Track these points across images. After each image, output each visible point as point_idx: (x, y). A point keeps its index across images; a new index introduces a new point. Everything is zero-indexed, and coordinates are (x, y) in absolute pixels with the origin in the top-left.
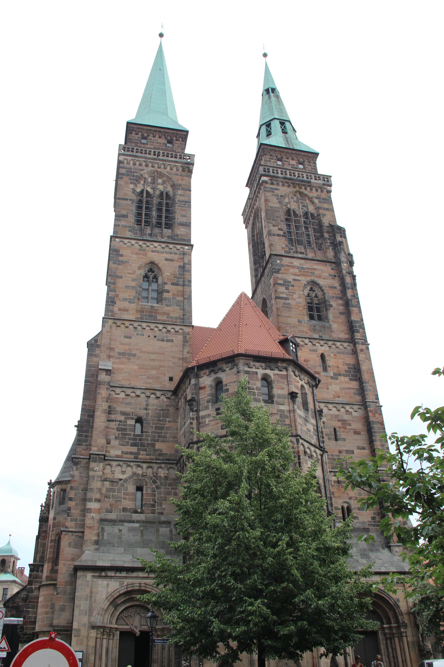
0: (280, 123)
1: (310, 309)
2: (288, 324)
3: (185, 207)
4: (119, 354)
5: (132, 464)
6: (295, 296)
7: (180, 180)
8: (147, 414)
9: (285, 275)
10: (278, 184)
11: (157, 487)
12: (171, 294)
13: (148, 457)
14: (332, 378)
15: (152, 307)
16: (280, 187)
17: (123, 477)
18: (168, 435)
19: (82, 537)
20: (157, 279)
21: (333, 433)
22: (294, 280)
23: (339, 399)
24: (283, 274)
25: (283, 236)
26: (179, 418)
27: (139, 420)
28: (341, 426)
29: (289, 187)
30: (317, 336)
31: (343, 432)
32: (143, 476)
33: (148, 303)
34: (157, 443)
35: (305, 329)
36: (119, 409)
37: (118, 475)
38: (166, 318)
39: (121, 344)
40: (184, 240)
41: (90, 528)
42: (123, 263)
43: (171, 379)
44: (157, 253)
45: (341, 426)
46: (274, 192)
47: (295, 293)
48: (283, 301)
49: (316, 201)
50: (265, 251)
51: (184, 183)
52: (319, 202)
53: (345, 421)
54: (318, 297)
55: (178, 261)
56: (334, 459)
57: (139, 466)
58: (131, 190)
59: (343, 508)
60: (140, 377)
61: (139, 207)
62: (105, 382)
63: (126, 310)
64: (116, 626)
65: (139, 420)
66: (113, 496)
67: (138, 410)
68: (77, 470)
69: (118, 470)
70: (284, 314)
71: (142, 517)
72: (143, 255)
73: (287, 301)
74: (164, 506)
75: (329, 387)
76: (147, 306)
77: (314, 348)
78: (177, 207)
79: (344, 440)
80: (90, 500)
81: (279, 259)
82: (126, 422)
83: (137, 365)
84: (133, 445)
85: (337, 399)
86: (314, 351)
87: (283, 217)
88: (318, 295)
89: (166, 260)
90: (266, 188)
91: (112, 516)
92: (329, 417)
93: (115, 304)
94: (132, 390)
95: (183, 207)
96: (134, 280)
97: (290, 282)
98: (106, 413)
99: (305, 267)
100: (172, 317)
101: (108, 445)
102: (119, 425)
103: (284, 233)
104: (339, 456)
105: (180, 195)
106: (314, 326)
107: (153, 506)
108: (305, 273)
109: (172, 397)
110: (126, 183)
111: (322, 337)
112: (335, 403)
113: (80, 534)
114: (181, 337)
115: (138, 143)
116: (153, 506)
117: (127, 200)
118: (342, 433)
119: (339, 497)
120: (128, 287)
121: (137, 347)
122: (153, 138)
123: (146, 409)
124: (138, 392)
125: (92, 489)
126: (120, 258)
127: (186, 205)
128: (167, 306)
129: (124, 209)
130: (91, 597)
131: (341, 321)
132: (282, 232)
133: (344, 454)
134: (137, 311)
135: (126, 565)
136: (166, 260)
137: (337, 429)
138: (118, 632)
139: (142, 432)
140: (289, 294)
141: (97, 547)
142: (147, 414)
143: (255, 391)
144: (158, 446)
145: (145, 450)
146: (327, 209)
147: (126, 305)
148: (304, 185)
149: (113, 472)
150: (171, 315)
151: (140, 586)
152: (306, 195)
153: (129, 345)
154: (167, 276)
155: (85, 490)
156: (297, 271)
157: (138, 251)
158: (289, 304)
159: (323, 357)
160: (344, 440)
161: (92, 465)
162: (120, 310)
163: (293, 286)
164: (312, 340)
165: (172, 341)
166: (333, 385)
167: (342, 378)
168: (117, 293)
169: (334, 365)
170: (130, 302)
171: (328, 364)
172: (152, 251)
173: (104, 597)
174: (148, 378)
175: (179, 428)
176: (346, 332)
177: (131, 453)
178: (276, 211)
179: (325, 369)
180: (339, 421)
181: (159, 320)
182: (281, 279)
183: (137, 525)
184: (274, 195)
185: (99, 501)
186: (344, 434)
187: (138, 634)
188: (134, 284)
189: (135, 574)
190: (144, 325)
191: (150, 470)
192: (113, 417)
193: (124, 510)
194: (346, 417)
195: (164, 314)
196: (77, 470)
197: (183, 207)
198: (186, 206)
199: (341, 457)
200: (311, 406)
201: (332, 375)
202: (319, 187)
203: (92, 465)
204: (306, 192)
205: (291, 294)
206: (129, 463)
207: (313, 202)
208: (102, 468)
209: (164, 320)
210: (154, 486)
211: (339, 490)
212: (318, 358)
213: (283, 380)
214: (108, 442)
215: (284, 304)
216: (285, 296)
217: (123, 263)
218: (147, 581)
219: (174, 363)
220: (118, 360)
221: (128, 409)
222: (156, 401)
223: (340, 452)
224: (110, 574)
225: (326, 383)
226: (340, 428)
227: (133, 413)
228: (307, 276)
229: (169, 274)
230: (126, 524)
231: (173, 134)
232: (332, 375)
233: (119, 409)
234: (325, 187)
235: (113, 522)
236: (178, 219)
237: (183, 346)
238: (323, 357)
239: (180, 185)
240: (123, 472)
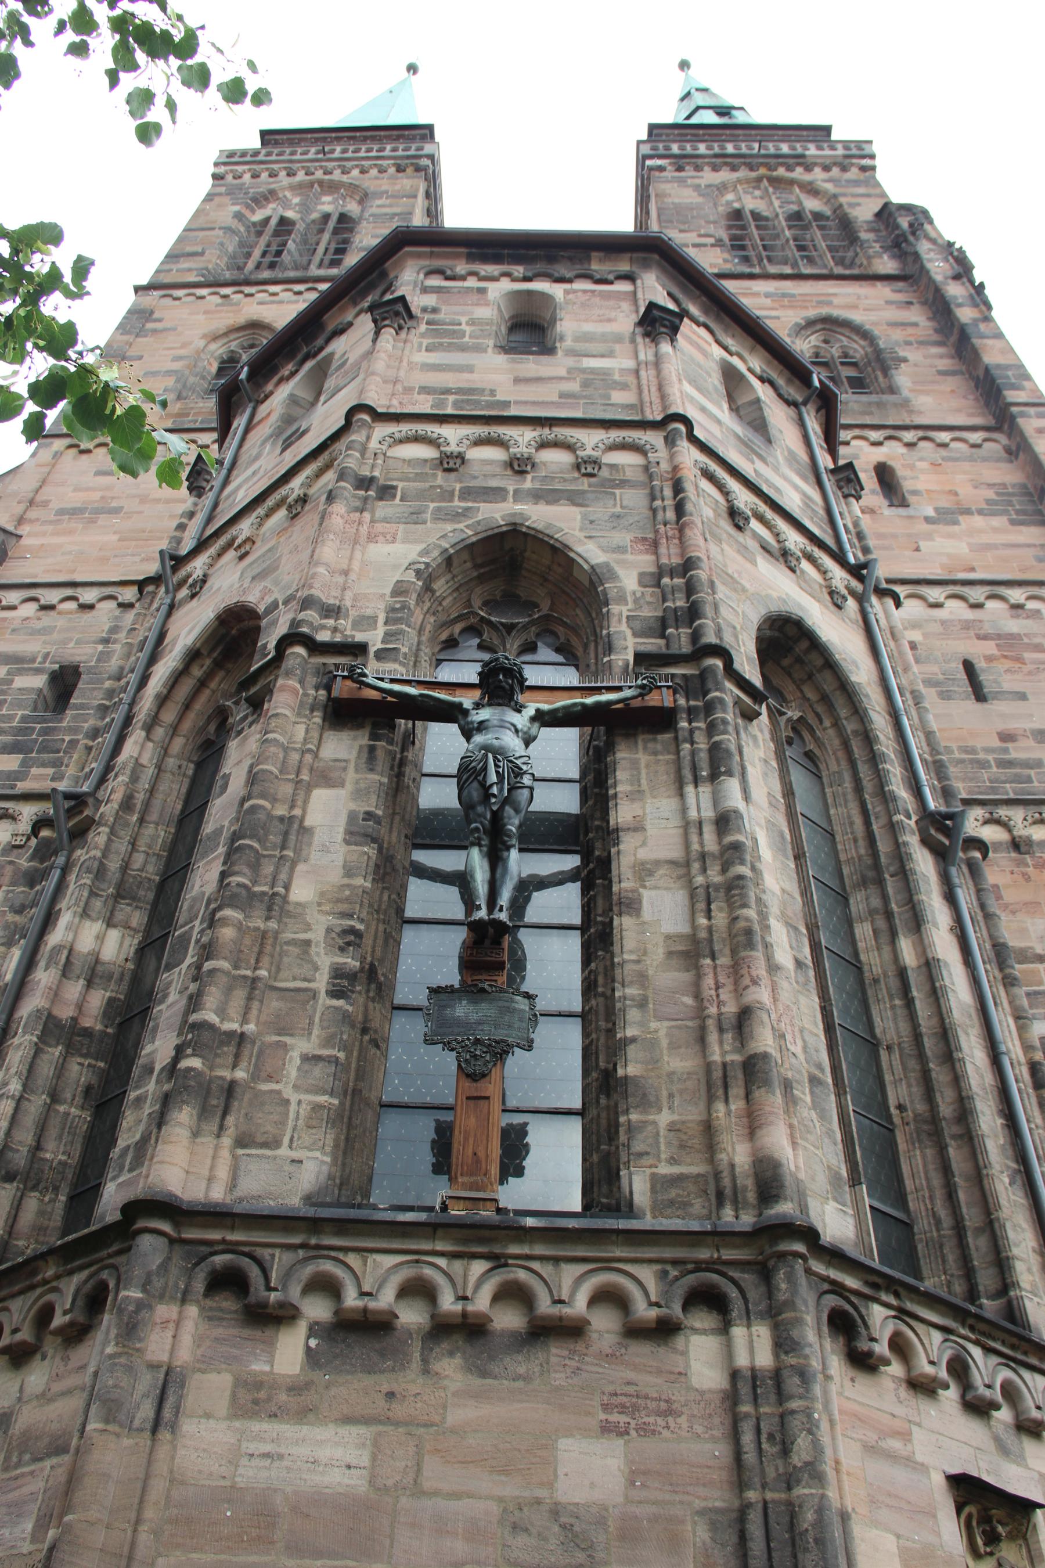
21: (963, 676)
25: (712, 245)
28: (995, 652)
45: (995, 652)
53: (1012, 636)
75: (922, 544)
79: (1022, 697)
104: (1006, 751)
112: (954, 582)
124: (88, 596)
131: (949, 389)
137: (980, 664)
152: (792, 182)
160: (1022, 697)
166: (938, 539)
167: (978, 521)
174: (142, 560)
186: (1016, 677)
194: (1014, 625)
199: (1013, 755)
211: (1027, 878)
223: (1007, 737)
226: (989, 659)
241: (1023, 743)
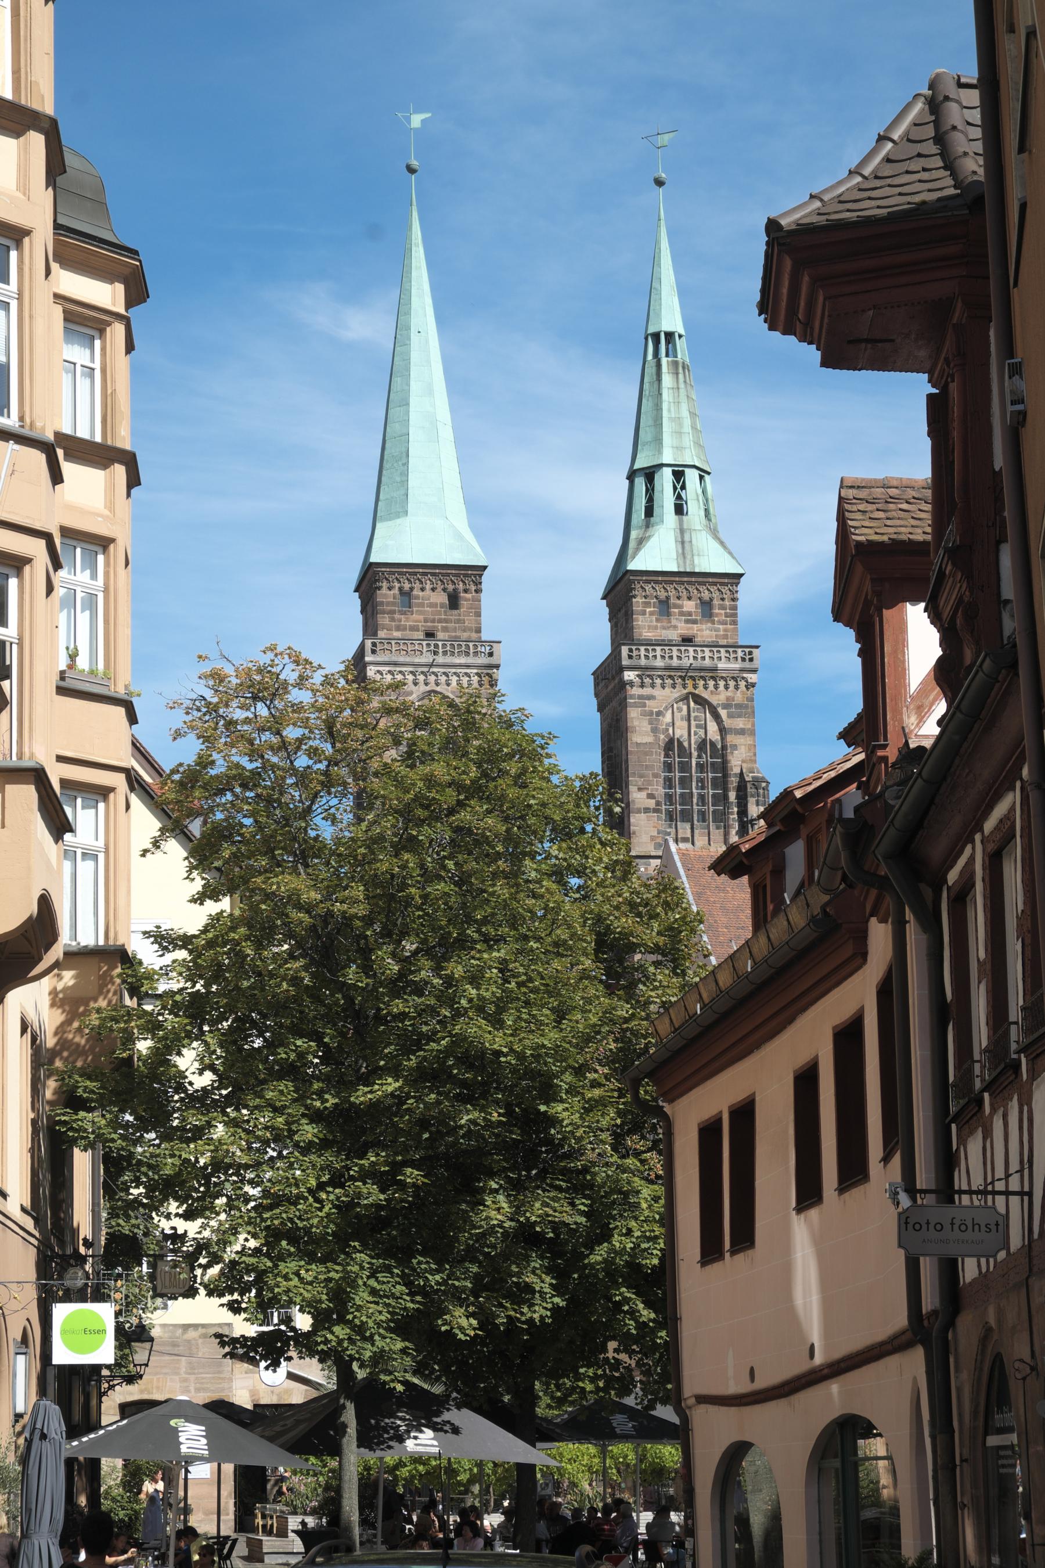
10: (653, 686)
16: (657, 692)
25: (655, 811)
29: (674, 688)
46: (644, 705)
49: (723, 713)
52: (730, 716)
81: (645, 864)
90: (632, 697)
103: (658, 803)
132: (653, 801)
146: (742, 732)
148: (703, 678)
184: (644, 714)
202: (733, 678)
204: (705, 695)
207: (717, 717)
234: (745, 675)
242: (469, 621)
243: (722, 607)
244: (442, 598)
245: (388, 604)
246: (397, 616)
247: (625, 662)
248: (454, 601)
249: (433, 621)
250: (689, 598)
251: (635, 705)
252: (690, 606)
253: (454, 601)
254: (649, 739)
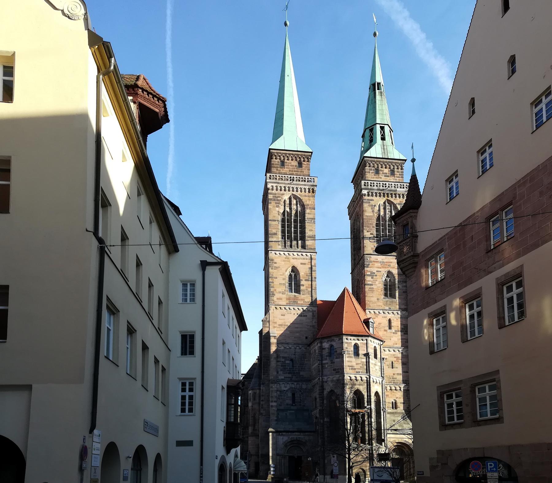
0: (381, 127)
1: (386, 289)
2: (371, 301)
3: (312, 223)
4: (279, 325)
5: (289, 383)
6: (377, 283)
7: (308, 201)
8: (295, 358)
9: (372, 268)
11: (302, 393)
12: (305, 287)
13: (297, 379)
14: (394, 333)
15: (295, 296)
17: (286, 389)
18: (306, 368)
19: (269, 417)
20: (296, 276)
22: (377, 271)
23: (396, 345)
24: (371, 267)
26: (311, 359)
27: (292, 360)
30: (387, 308)
31: (397, 363)
32: (295, 388)
33: (292, 292)
34: (301, 372)
35: (381, 304)
36: (281, 355)
37: (284, 389)
38: (302, 303)
39: (279, 319)
40: (311, 249)
41: (273, 414)
42: (276, 268)
43: (306, 338)
44: (296, 260)
46: (370, 203)
47: (377, 280)
48: (369, 286)
50: (361, 246)
51: (310, 203)
54: (391, 281)
55: (308, 265)
56: (390, 378)
57: (293, 384)
58: (277, 212)
59: (392, 402)
60: (291, 338)
61: (283, 226)
62: (274, 343)
63: (281, 299)
64: (287, 454)
65: (292, 360)
66: (281, 398)
67: (291, 355)
68: (264, 387)
69: (283, 386)
70: (369, 295)
71: (295, 408)
72: (288, 261)
73: (372, 287)
74: (305, 403)
76: (293, 295)
77: (385, 315)
78: (306, 224)
79: (397, 368)
80: (272, 402)
81: (369, 257)
82: (285, 362)
83: (289, 331)
84: (289, 373)
85: (395, 345)
86: (385, 317)
87: (375, 222)
88: (391, 280)
89: (301, 264)
90: (365, 200)
91: (282, 408)
92: (390, 356)
93: (275, 295)
94: (287, 345)
95: (310, 223)
96: (284, 279)
97: (374, 273)
98: (275, 359)
99: (385, 261)
100: (306, 302)
101: (278, 374)
102: (282, 364)
105: (308, 213)
106: (387, 302)
107: (300, 402)
108: (385, 266)
109: (308, 348)
110: (274, 207)
111: (390, 308)
113: (268, 416)
114: (311, 314)
115: (278, 167)
116: (300, 402)
117: (275, 221)
118: (396, 364)
119: (391, 397)
120: (281, 284)
121: (288, 321)
122: (288, 161)
123: (295, 355)
124: (290, 346)
125: (272, 397)
126: (275, 265)
127: (311, 221)
128: (303, 294)
129: (274, 229)
130: (276, 443)
133: (396, 375)
134: (287, 299)
135: (290, 430)
136: (301, 264)
137: (394, 362)
138: (288, 457)
139: (293, 366)
140: (373, 281)
141: (277, 422)
142: (295, 358)
143: (350, 352)
144: (301, 373)
145: (295, 376)
147: (280, 295)
149: (281, 387)
150: (305, 301)
151: (297, 439)
153: (284, 319)
154: (302, 275)
155: (268, 396)
156: (379, 265)
157: (285, 259)
158: (373, 288)
159: (390, 321)
160: (397, 368)
161: (271, 385)
162: (277, 299)
163: (376, 276)
164: (384, 311)
165: (306, 316)
168: (275, 288)
169: (396, 325)
170: (282, 294)
171: (392, 325)
172: (293, 259)
173: (282, 443)
175: (311, 364)
176: (405, 304)
177: (289, 377)
178: (370, 219)
179: (390, 328)
180: (395, 357)
181: (299, 304)
182: (369, 271)
183: (293, 411)
184: (369, 206)
185: (275, 402)
187: (296, 457)
188: (283, 282)
189: (294, 434)
190: (291, 308)
191: (298, 385)
192: (279, 359)
193: (287, 404)
195: (301, 300)
196: (264, 387)
197: (310, 223)
198: (312, 222)
200: (379, 356)
201: (394, 332)
203: (271, 385)
205: (375, 281)
206: (288, 382)
208: (276, 387)
209: (302, 304)
210: (300, 393)
211: (391, 394)
212: (387, 322)
213: (364, 346)
214: (278, 373)
215: (370, 288)
216: (370, 283)
217: (276, 268)
218: (299, 436)
219: (308, 329)
220: (278, 329)
221: (286, 355)
222: (299, 351)
223: (394, 374)
224: (284, 434)
225: (390, 336)
226: (395, 361)
227: (288, 357)
228: (386, 267)
229: (303, 274)
230: (288, 411)
231: (301, 155)
232: (394, 332)
233: (281, 355)
235: (282, 410)
236: (307, 233)
237: (313, 318)
238: (390, 321)
239: (308, 205)
240: (285, 387)
241: (395, 375)
242: (306, 172)
243: (398, 172)
244: (295, 163)
245: (276, 164)
246: (279, 169)
247: (363, 187)
248: (300, 164)
249: (292, 171)
250: (386, 168)
251: (366, 202)
252: (386, 171)
253: (300, 164)
254: (372, 214)
